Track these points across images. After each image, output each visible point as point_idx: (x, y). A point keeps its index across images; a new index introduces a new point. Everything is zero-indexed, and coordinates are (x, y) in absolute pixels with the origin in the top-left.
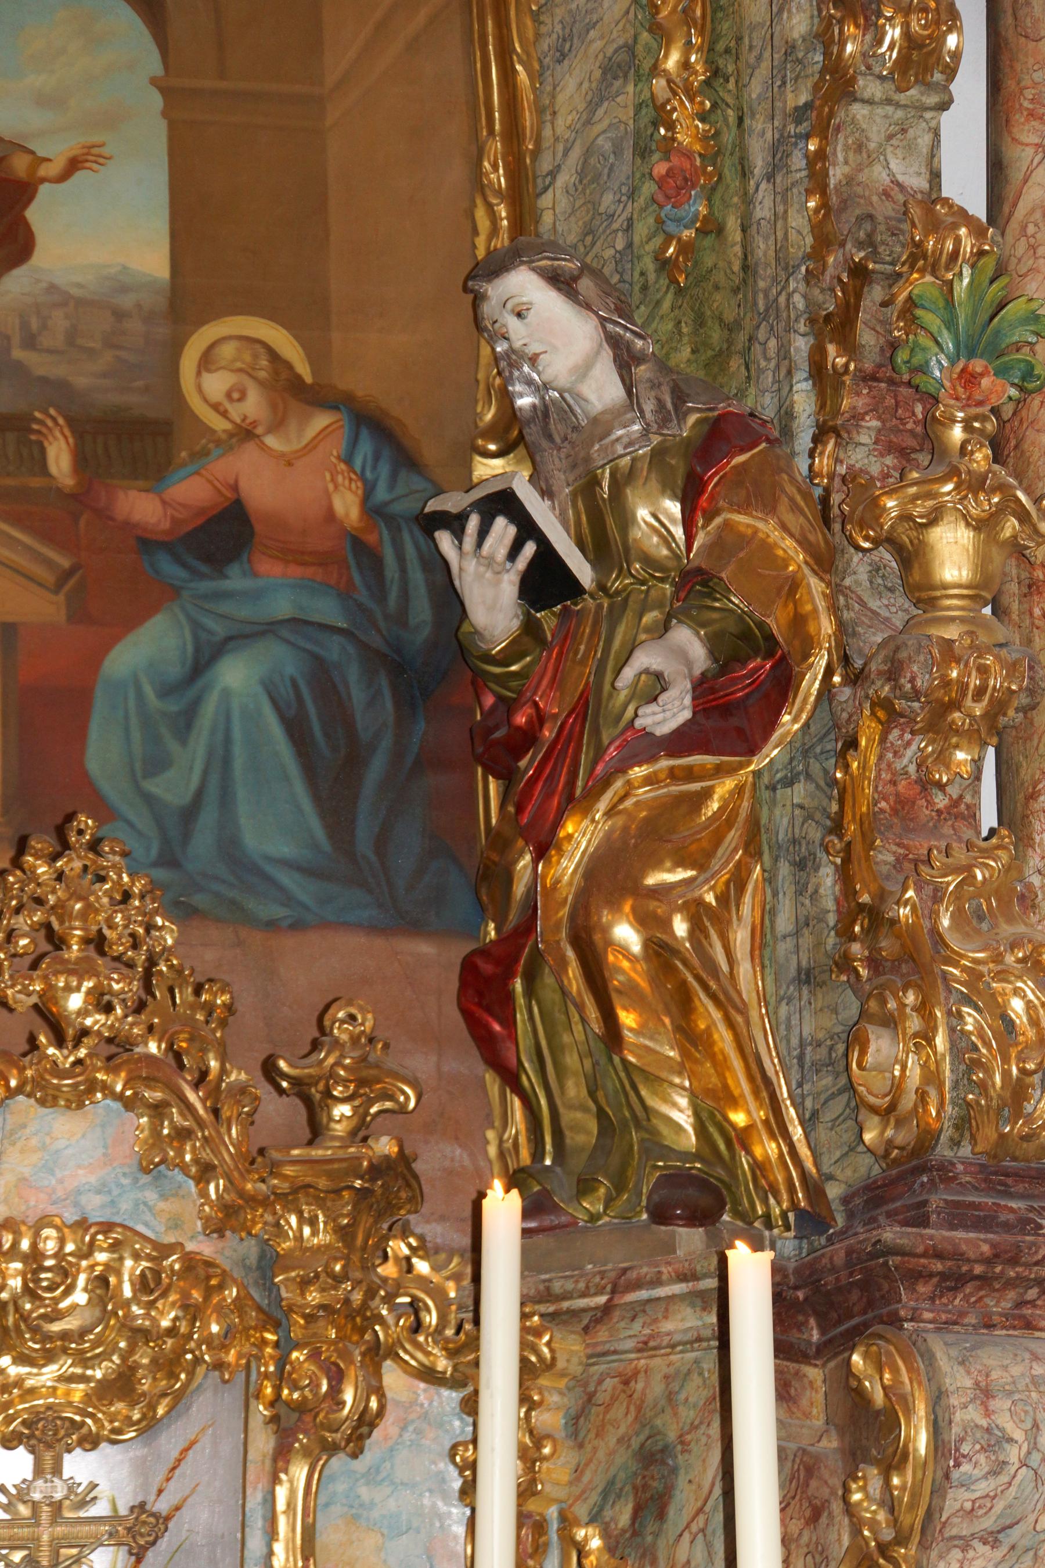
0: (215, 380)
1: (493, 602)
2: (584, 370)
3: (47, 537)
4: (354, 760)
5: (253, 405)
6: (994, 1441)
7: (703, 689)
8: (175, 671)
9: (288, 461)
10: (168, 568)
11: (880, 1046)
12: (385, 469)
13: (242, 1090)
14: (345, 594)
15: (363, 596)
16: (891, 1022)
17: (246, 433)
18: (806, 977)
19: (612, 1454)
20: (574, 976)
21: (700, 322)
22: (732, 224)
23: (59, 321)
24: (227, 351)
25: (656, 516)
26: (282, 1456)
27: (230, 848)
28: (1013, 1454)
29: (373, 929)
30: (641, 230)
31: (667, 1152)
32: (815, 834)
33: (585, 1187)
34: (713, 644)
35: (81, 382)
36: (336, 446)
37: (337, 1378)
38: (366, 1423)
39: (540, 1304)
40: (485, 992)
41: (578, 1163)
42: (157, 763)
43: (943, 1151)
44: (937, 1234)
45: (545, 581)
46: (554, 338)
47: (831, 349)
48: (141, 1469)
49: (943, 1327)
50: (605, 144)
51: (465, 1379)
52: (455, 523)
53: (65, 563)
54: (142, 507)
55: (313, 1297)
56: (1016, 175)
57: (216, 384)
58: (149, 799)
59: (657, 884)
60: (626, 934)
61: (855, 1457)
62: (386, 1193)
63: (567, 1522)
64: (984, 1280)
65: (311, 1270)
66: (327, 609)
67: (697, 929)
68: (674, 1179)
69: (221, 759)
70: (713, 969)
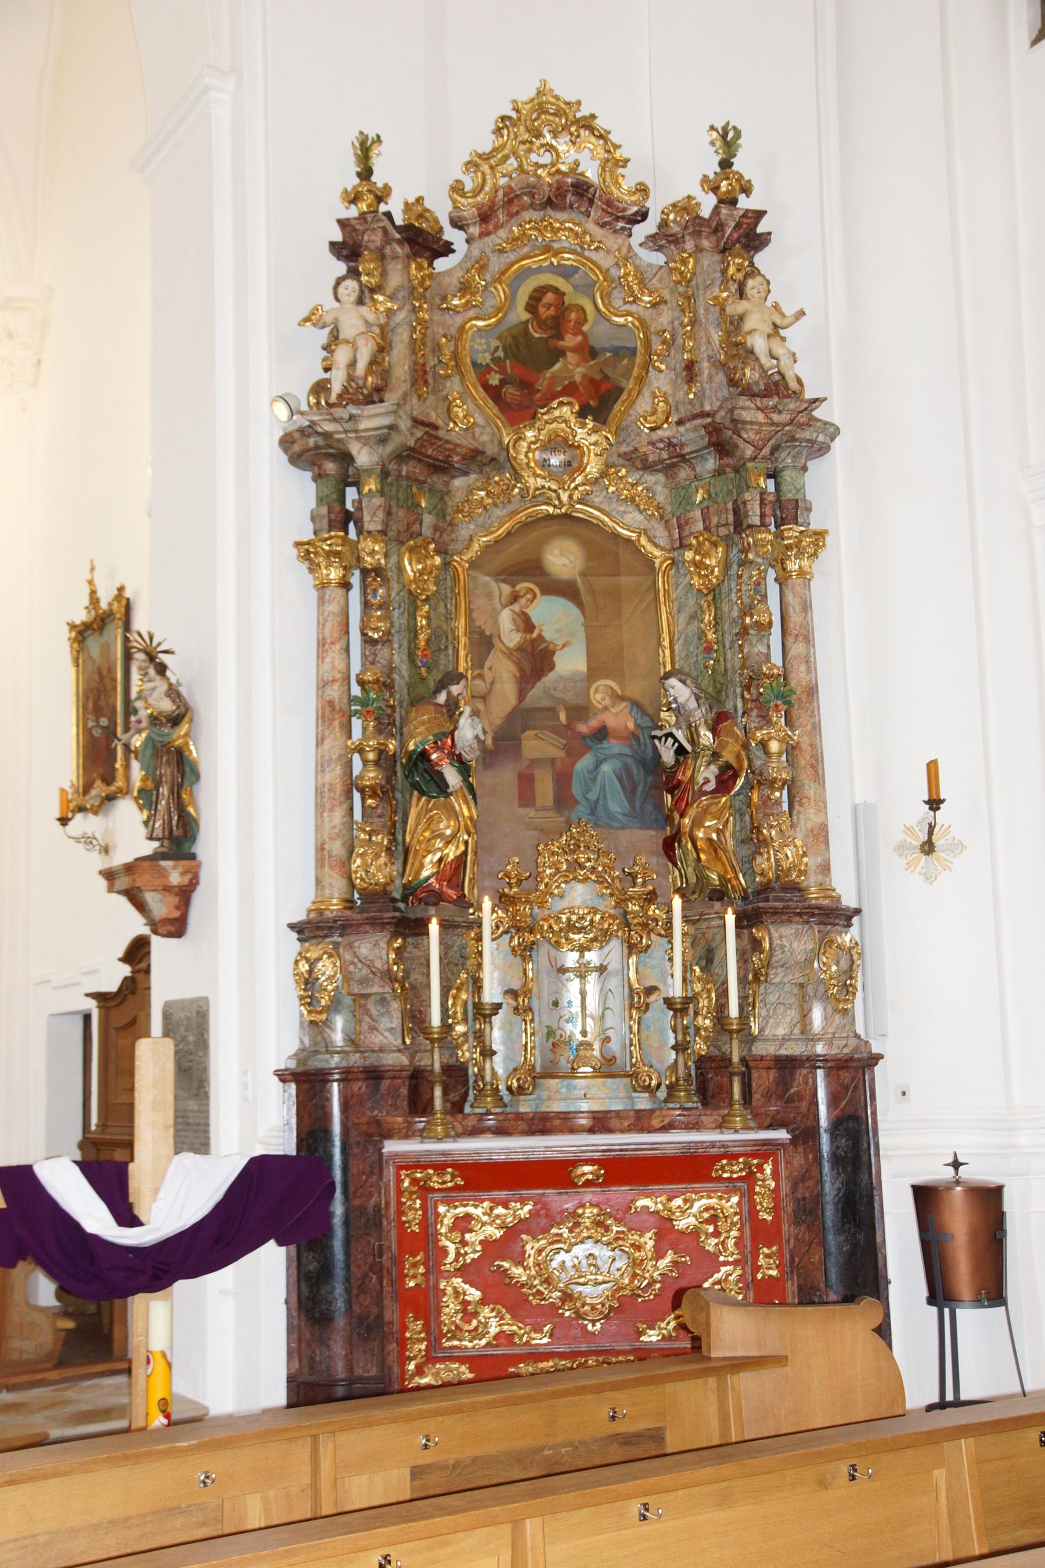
0: (598, 697)
1: (668, 756)
2: (688, 700)
3: (561, 736)
4: (634, 791)
5: (607, 701)
6: (782, 947)
7: (717, 777)
8: (591, 767)
9: (616, 714)
10: (590, 743)
11: (759, 859)
12: (639, 715)
13: (618, 877)
14: (631, 746)
15: (635, 747)
16: (761, 854)
17: (606, 708)
18: (743, 841)
19: (701, 950)
20: (690, 846)
21: (714, 681)
22: (722, 659)
23: (562, 684)
24: (601, 688)
25: (706, 737)
26: (630, 954)
27: (606, 809)
28: (786, 949)
29: (641, 828)
30: (700, 658)
31: (712, 885)
32: (744, 807)
33: (694, 893)
34: (720, 768)
35: (567, 698)
36: (627, 710)
37: (642, 938)
38: (648, 946)
39: (686, 919)
40: (669, 847)
41: (692, 886)
42: (588, 790)
43: (773, 884)
44: (770, 904)
45: (681, 751)
46: (680, 691)
47: (746, 693)
48: (600, 956)
49: (772, 923)
50: (690, 634)
51: (669, 935)
52: (660, 739)
53: (564, 742)
54: (583, 728)
55: (636, 921)
56: (787, 648)
57: (599, 696)
58: (587, 799)
59: (709, 825)
60: (700, 834)
61: (754, 950)
62: (651, 897)
63: (691, 965)
64: (782, 913)
65: (636, 915)
66: (627, 751)
67: (718, 835)
68: (714, 891)
69: (603, 788)
70: (721, 842)
